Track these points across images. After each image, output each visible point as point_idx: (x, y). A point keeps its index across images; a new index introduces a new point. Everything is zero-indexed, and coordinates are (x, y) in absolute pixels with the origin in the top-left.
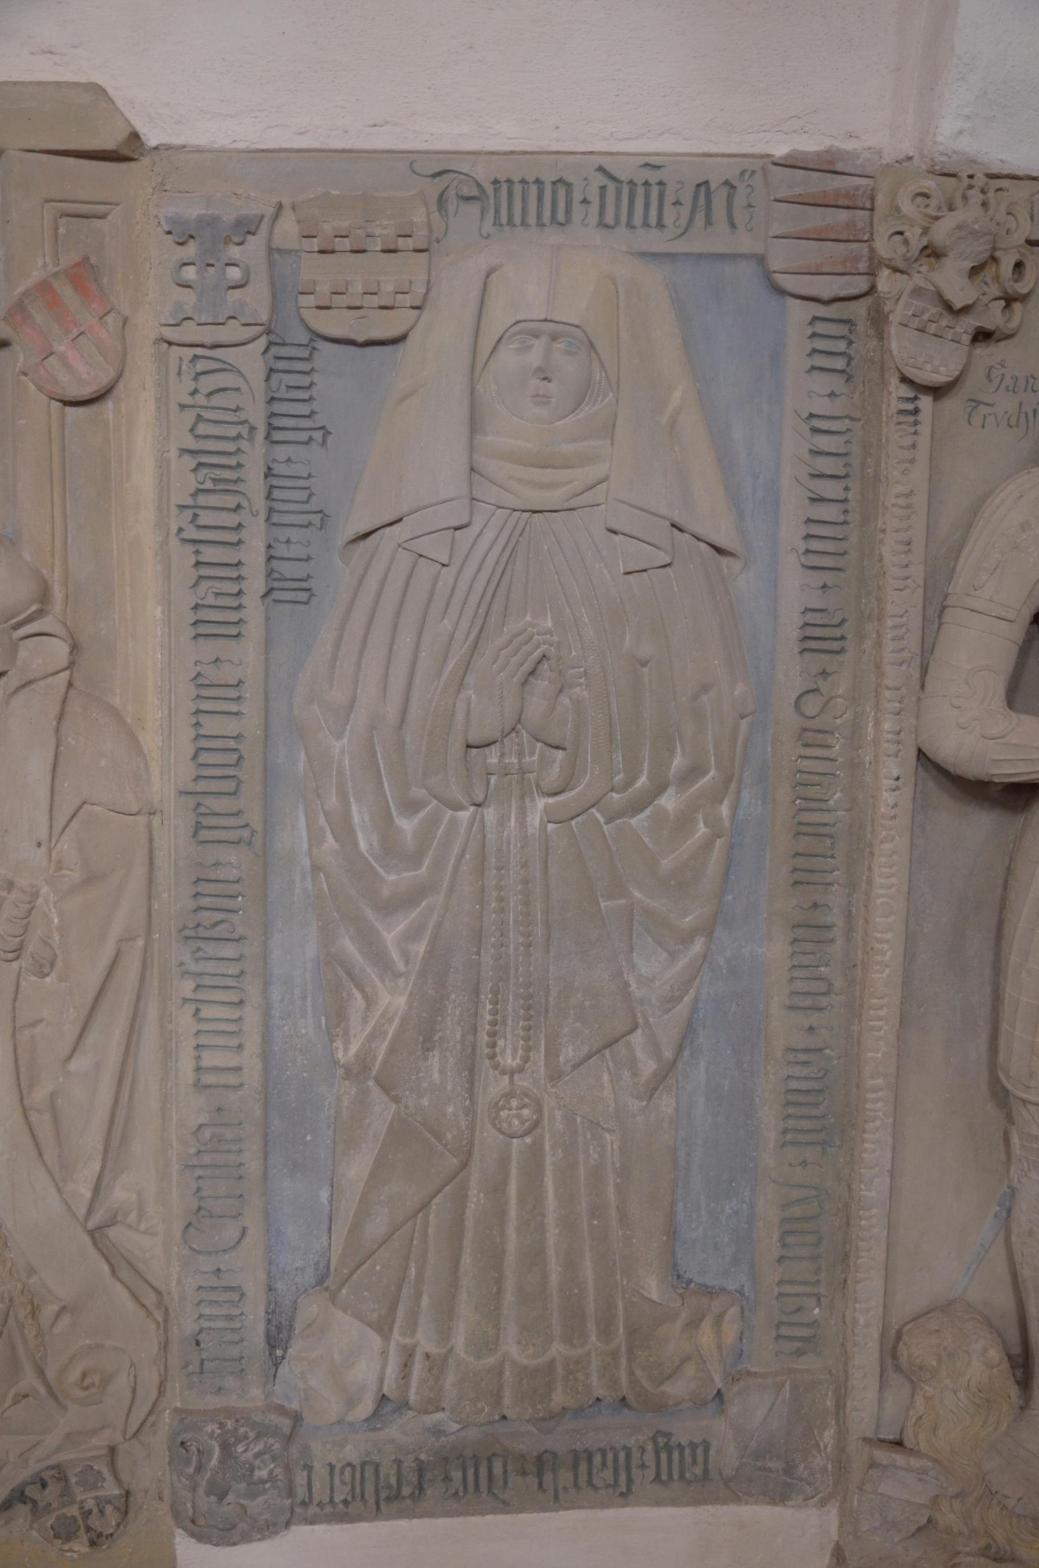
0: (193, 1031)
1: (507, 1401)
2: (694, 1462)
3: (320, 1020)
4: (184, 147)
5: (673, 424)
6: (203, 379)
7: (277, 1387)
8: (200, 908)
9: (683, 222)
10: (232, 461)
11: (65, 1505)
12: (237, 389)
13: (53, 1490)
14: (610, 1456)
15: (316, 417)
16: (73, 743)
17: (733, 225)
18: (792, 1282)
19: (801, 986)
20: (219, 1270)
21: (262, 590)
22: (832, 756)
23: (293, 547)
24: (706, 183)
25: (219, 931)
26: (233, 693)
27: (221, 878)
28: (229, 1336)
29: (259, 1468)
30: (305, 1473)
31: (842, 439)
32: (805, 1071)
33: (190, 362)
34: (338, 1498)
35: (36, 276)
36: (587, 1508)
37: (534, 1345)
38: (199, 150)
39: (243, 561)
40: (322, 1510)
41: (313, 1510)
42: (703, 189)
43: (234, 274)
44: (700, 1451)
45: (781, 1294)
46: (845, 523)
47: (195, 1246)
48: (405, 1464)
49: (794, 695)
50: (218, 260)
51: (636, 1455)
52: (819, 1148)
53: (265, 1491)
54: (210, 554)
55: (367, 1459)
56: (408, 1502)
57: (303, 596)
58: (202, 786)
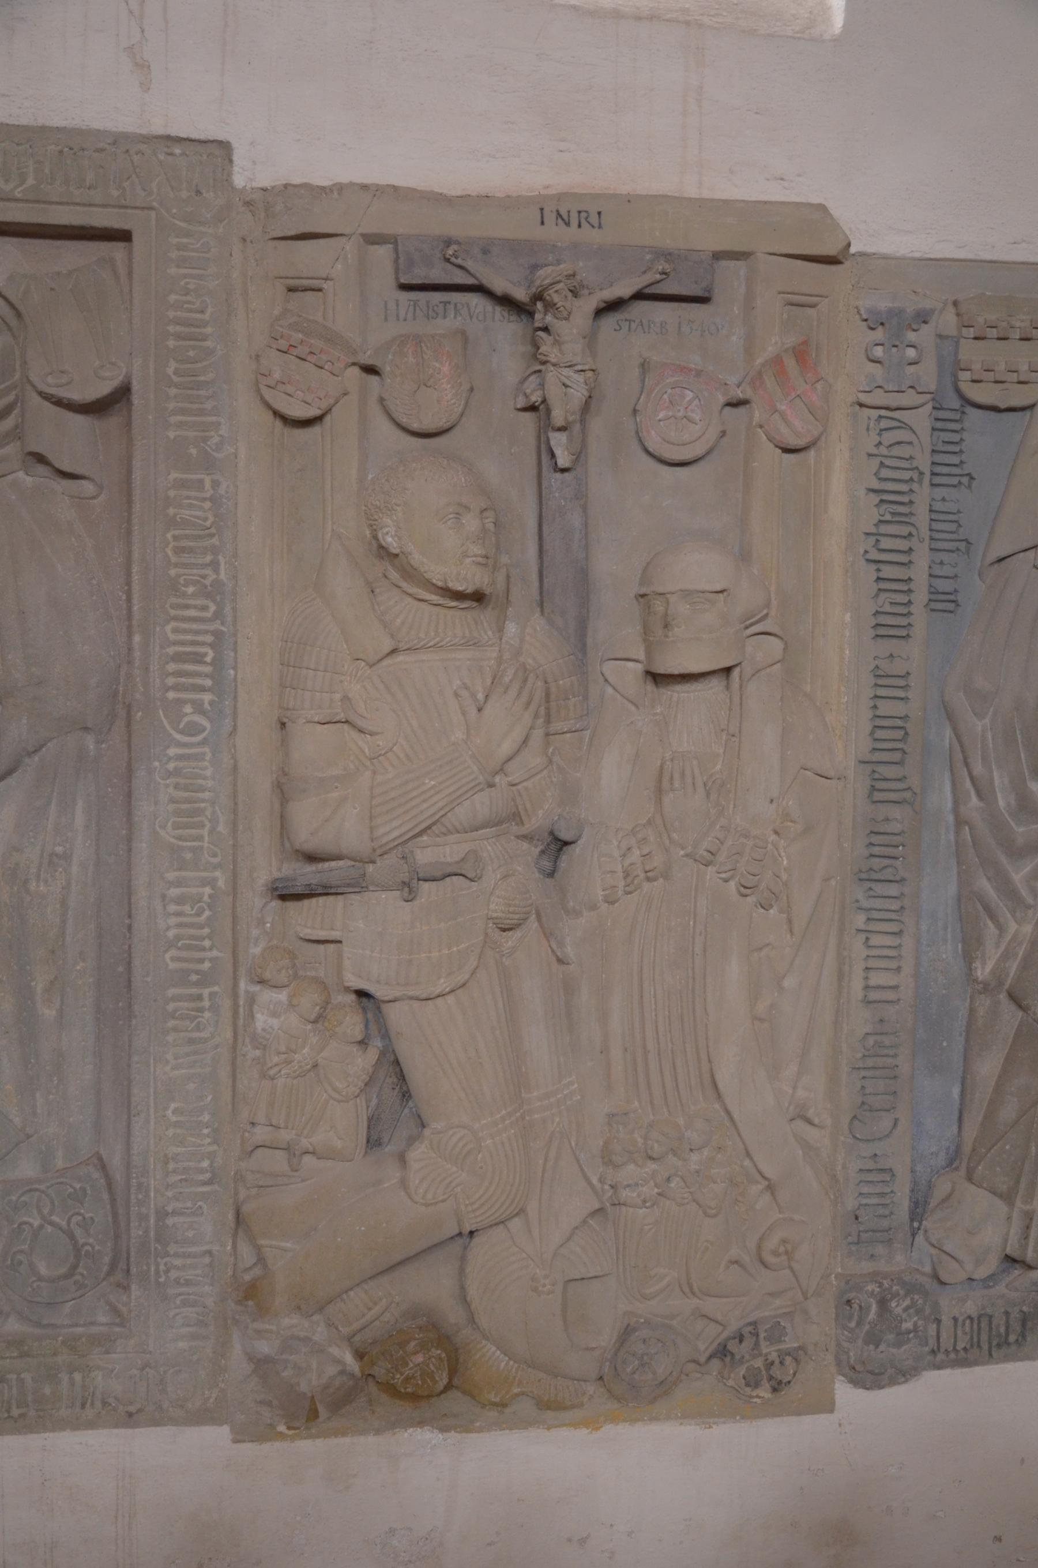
0: (864, 956)
3: (957, 946)
4: (874, 254)
6: (885, 434)
7: (913, 1254)
8: (872, 856)
10: (905, 499)
11: (754, 1357)
12: (910, 443)
13: (749, 1343)
15: (965, 466)
16: (791, 720)
20: (876, 1155)
21: (926, 601)
23: (945, 567)
25: (888, 874)
26: (901, 682)
27: (889, 831)
28: (881, 1211)
29: (906, 1321)
30: (935, 1326)
33: (876, 420)
34: (960, 1346)
35: (771, 351)
38: (885, 257)
39: (912, 577)
40: (947, 1356)
41: (940, 1357)
43: (911, 353)
47: (858, 1136)
48: (1012, 1316)
50: (902, 343)
53: (909, 1340)
54: (888, 571)
55: (983, 1312)
56: (1014, 1347)
57: (951, 606)
58: (878, 756)
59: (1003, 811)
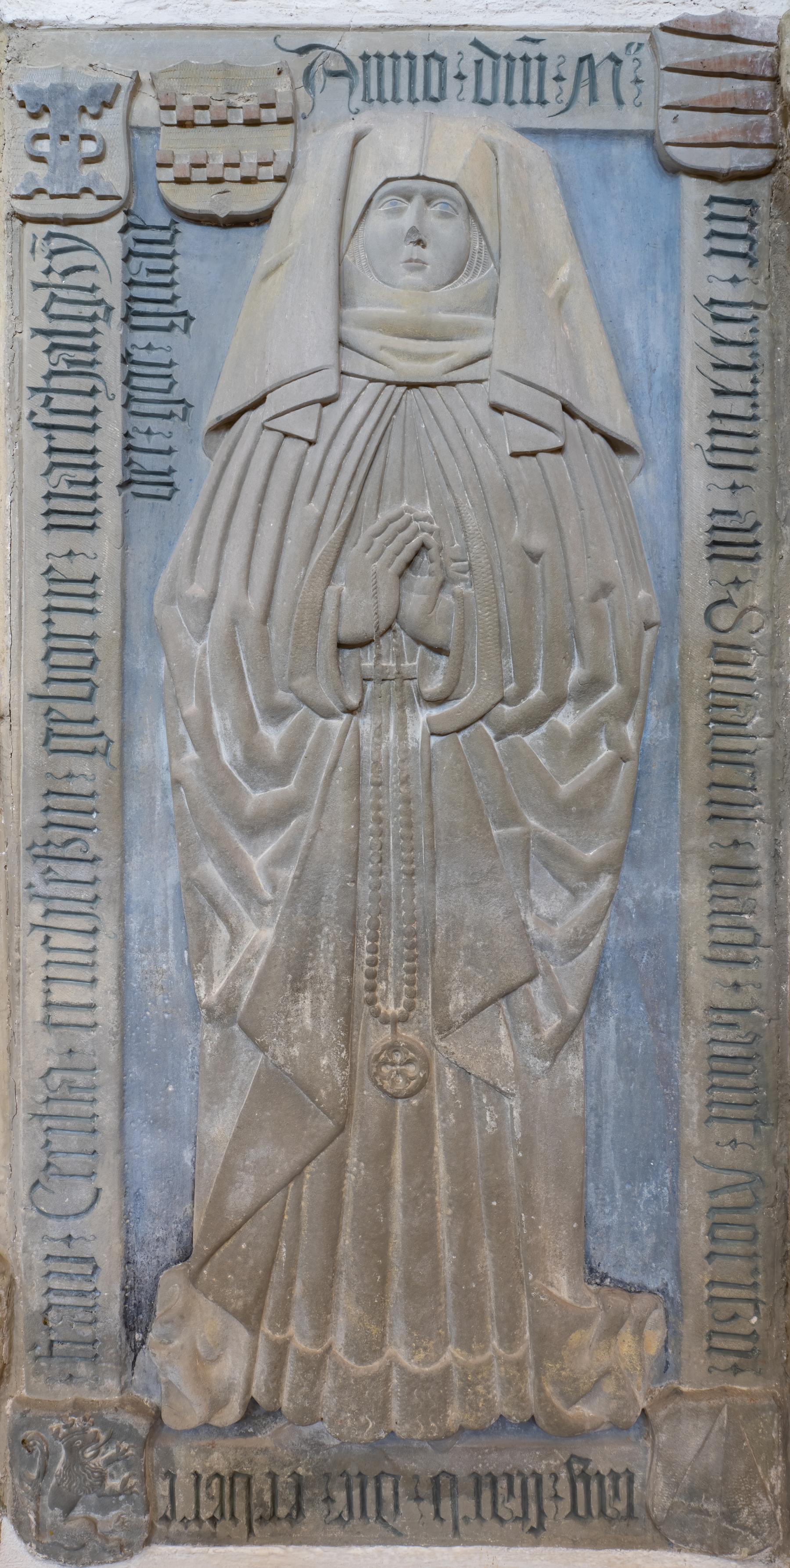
0: (43, 960)
1: (395, 1414)
2: (616, 1495)
3: (182, 955)
4: (41, 24)
5: (561, 301)
6: (58, 258)
7: (136, 1377)
8: (50, 824)
9: (566, 97)
10: (87, 342)
12: (93, 268)
14: (517, 1482)
15: (178, 301)
17: (620, 102)
18: (724, 1284)
19: (722, 935)
20: (70, 1237)
21: (118, 478)
22: (750, 675)
23: (153, 437)
24: (590, 57)
25: (71, 851)
26: (87, 589)
27: (74, 791)
28: (81, 1315)
29: (112, 1476)
30: (167, 1483)
31: (747, 327)
32: (731, 1034)
33: (44, 239)
34: (205, 1514)
36: (492, 1544)
37: (425, 1349)
38: (57, 28)
39: (98, 447)
40: (186, 1528)
41: (175, 1527)
42: (586, 63)
43: (89, 148)
44: (622, 1483)
45: (712, 1298)
46: (754, 418)
47: (42, 1208)
48: (281, 1480)
49: (704, 606)
50: (73, 132)
51: (547, 1483)
52: (750, 1126)
53: (118, 1505)
54: (63, 439)
55: (237, 1470)
56: (285, 1525)
57: (165, 491)
58: (55, 689)
59: (230, 767)
